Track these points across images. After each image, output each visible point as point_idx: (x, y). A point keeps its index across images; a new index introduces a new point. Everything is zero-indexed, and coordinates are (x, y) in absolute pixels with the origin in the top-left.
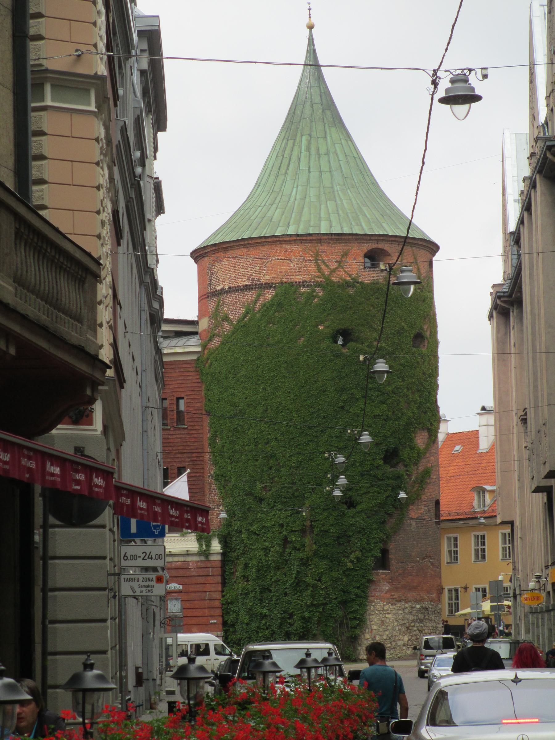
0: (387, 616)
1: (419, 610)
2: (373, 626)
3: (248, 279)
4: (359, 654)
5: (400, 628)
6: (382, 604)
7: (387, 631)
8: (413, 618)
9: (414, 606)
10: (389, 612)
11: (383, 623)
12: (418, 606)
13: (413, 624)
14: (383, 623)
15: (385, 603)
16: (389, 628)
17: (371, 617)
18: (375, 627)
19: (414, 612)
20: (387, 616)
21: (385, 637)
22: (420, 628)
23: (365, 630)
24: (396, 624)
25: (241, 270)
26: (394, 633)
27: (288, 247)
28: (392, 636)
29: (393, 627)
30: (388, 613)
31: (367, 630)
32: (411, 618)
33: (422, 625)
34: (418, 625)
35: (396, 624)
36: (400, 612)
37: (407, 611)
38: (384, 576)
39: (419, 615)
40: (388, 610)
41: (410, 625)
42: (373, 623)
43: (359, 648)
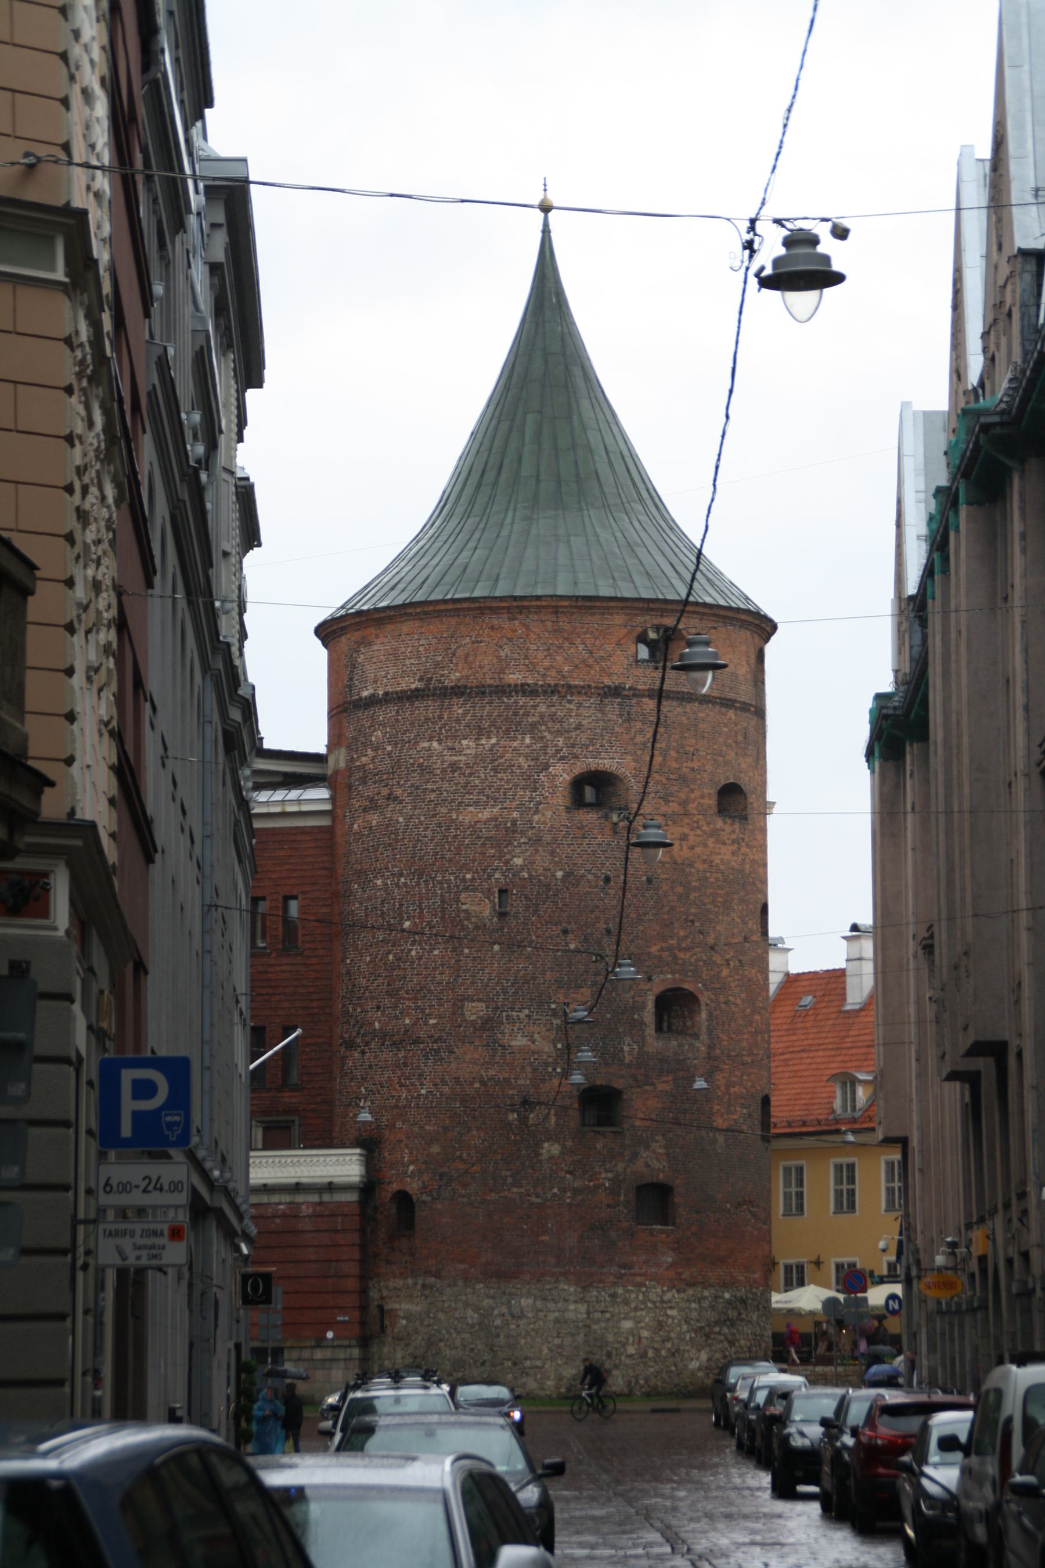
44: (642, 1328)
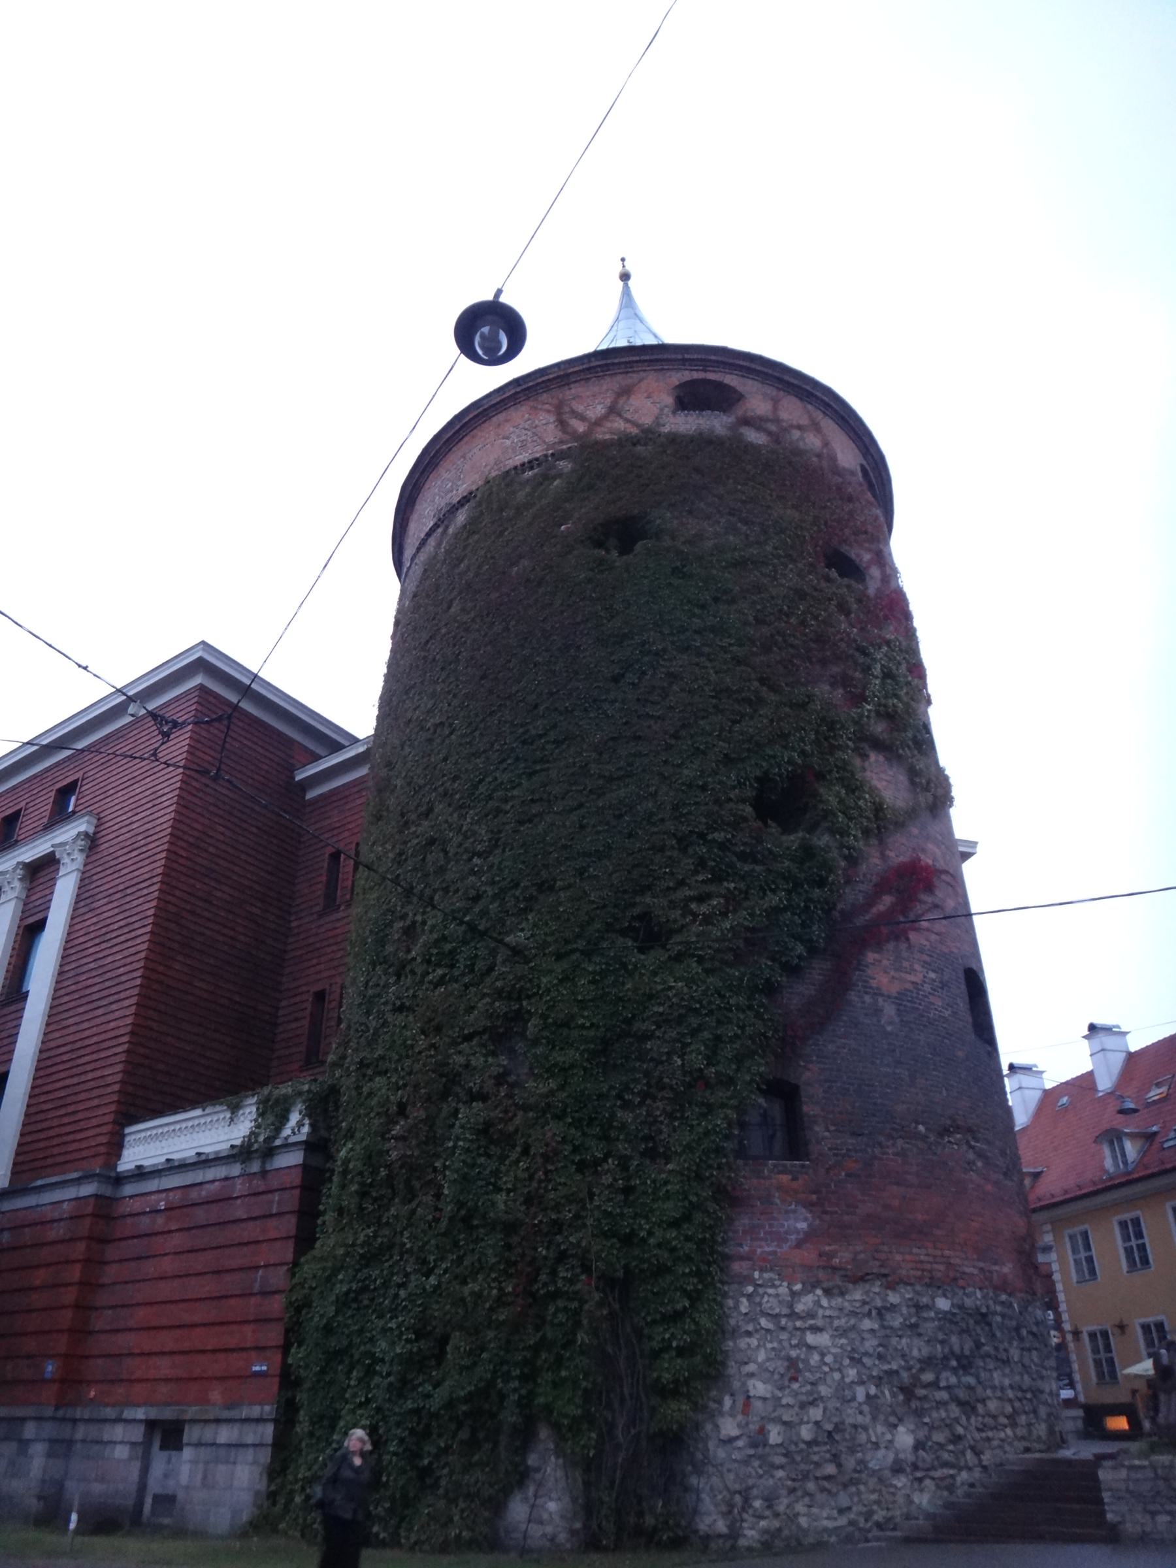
0: (811, 1338)
1: (947, 1318)
2: (751, 1383)
4: (695, 1511)
5: (873, 1390)
6: (783, 1290)
7: (813, 1403)
8: (925, 1351)
9: (925, 1300)
10: (819, 1322)
11: (794, 1369)
12: (943, 1304)
13: (928, 1377)
14: (794, 1369)
15: (798, 1287)
16: (824, 1390)
17: (743, 1343)
18: (759, 1388)
19: (929, 1327)
20: (811, 1338)
22: (962, 1394)
23: (720, 1402)
24: (852, 1373)
26: (851, 1416)
28: (839, 1428)
29: (841, 1386)
30: (816, 1329)
31: (728, 1402)
32: (918, 1349)
33: (971, 1380)
34: (953, 1380)
35: (852, 1373)
36: (867, 1324)
37: (897, 1321)
38: (785, 1178)
39: (954, 1339)
40: (811, 1315)
41: (916, 1378)
42: (752, 1367)
43: (694, 1480)
44: (751, 1375)
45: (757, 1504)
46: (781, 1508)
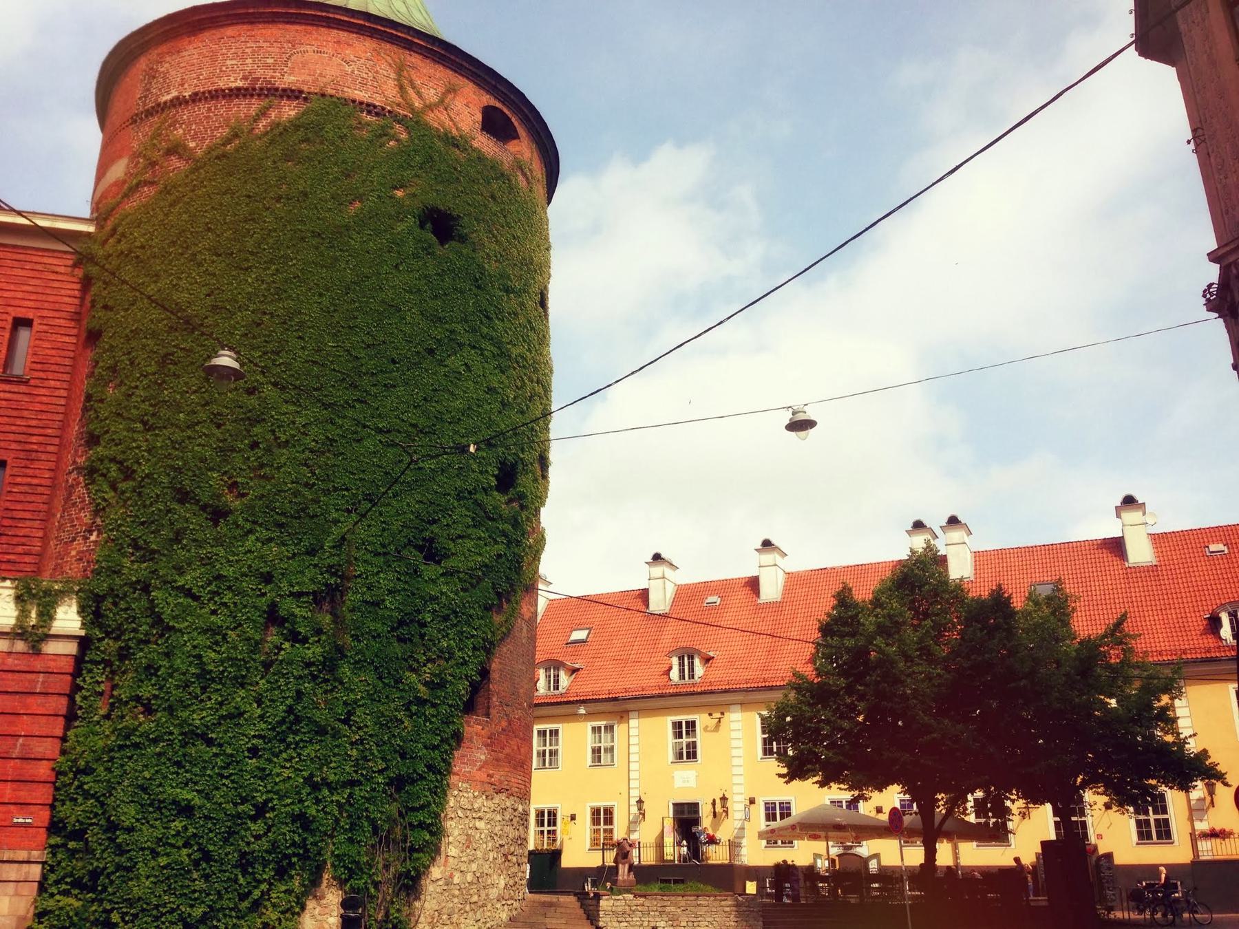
3: (245, 78)
21: (469, 878)
25: (229, 62)
27: (343, 35)
45: (444, 917)
46: (454, 920)
